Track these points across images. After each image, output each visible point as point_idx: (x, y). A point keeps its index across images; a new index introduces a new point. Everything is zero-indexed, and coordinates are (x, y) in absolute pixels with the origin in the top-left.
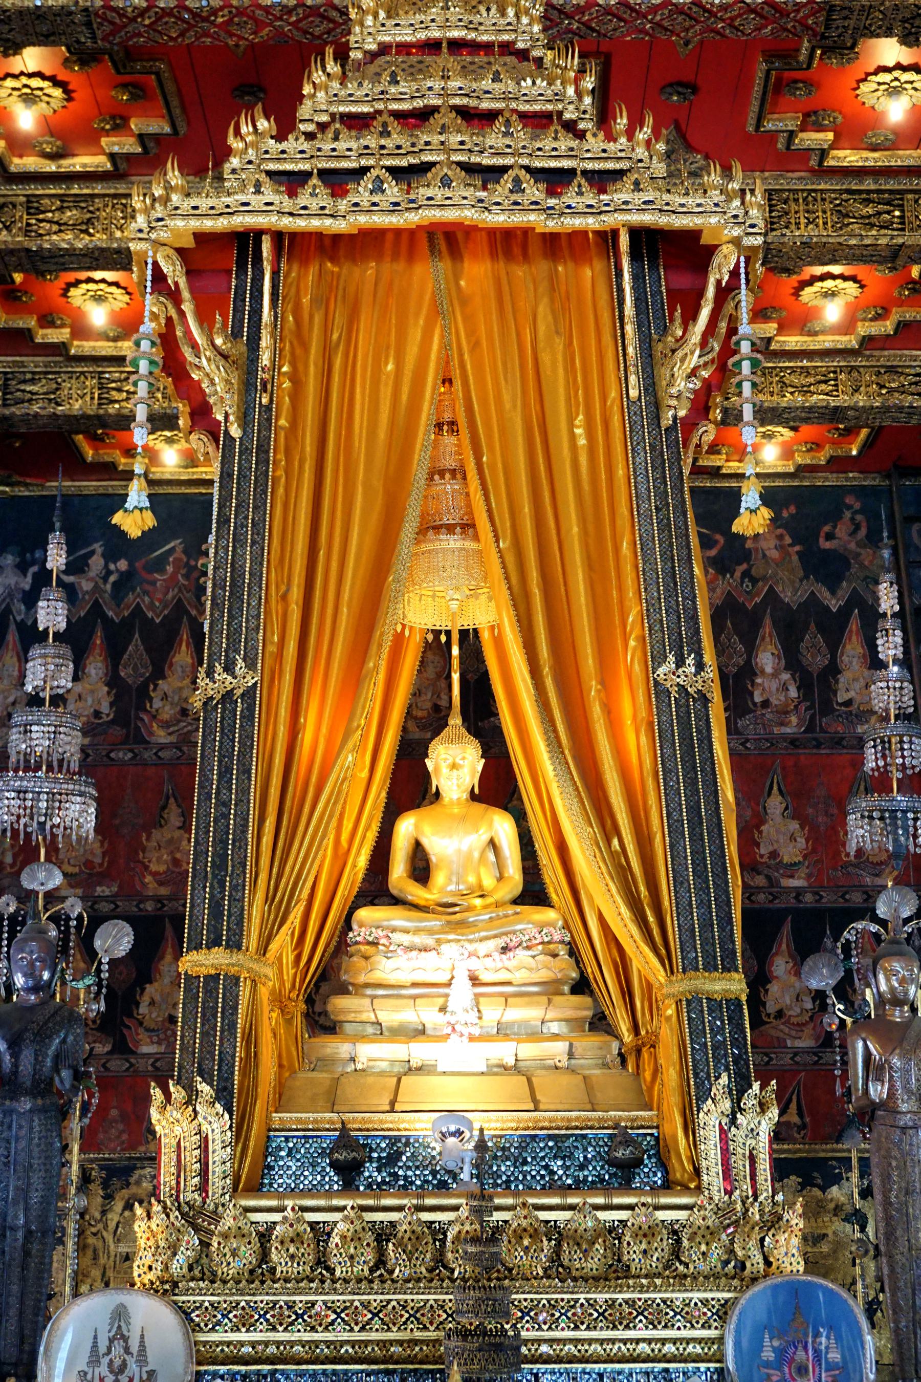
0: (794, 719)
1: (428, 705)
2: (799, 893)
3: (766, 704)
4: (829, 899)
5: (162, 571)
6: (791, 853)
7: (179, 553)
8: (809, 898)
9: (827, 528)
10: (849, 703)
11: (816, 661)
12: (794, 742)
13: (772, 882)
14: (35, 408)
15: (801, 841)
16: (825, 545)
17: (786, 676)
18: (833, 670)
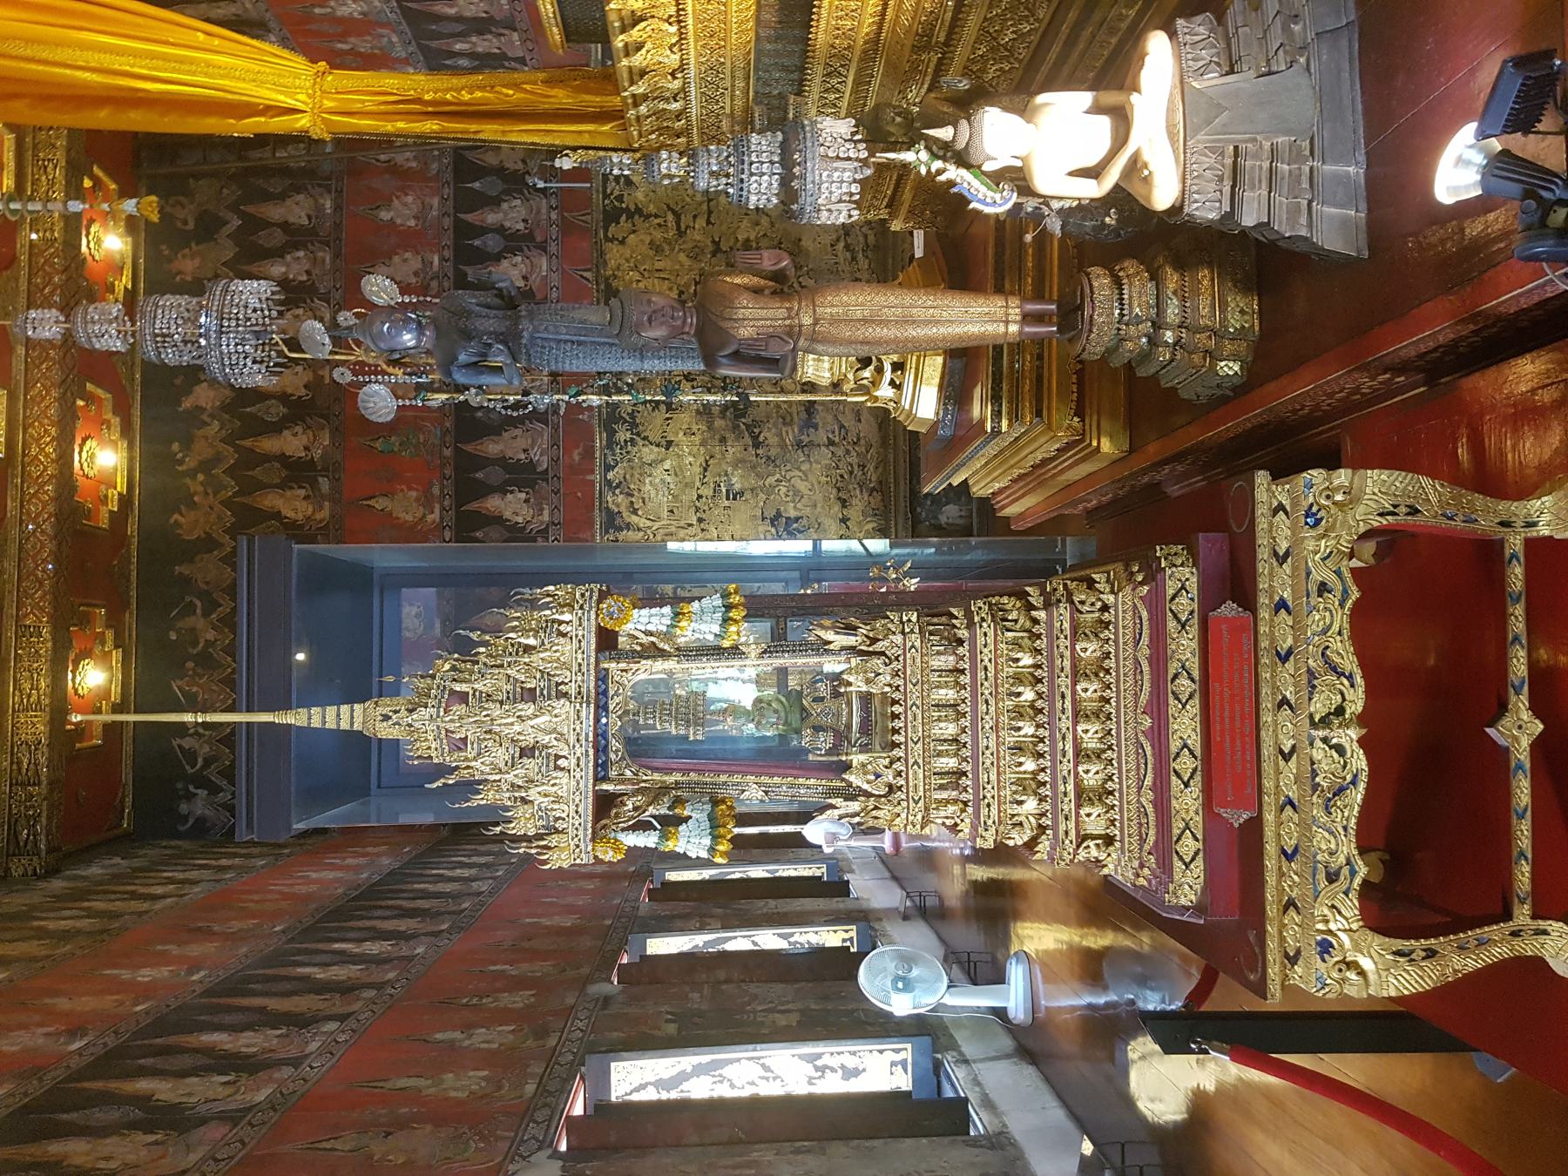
0: (320, 254)
1: (304, 503)
2: (443, 259)
3: (308, 272)
4: (448, 240)
5: (195, 695)
6: (415, 263)
7: (179, 683)
8: (446, 253)
9: (179, 224)
10: (309, 217)
11: (278, 238)
12: (337, 256)
13: (435, 277)
14: (43, 760)
15: (407, 255)
16: (191, 226)
17: (288, 257)
18: (285, 226)
